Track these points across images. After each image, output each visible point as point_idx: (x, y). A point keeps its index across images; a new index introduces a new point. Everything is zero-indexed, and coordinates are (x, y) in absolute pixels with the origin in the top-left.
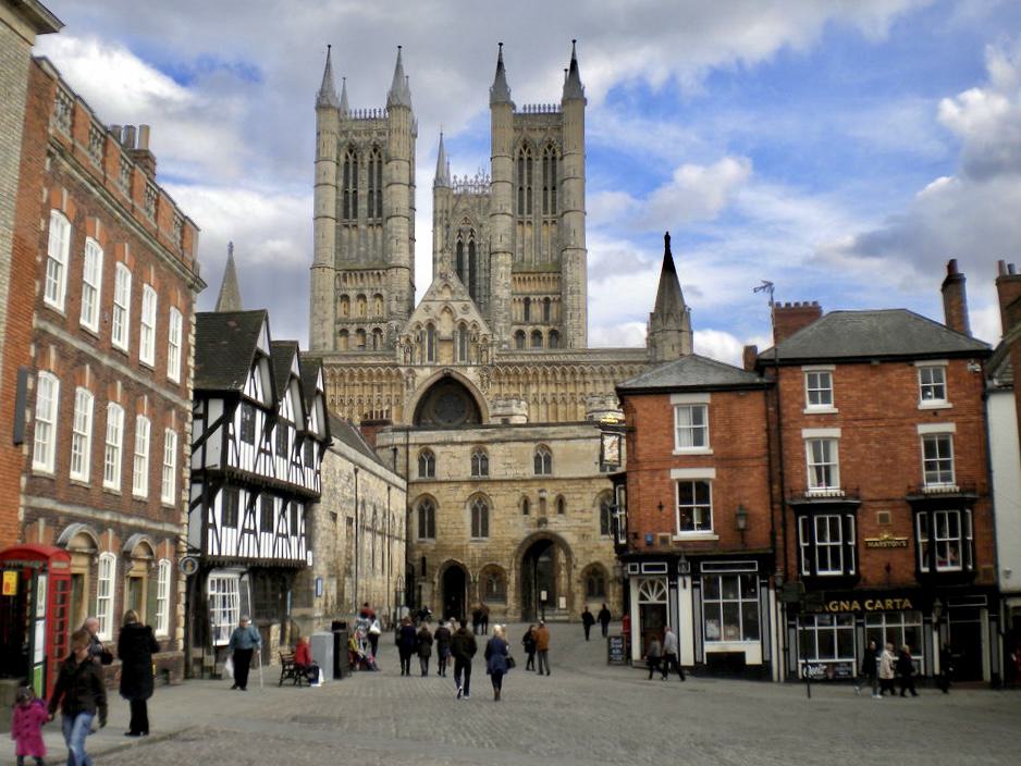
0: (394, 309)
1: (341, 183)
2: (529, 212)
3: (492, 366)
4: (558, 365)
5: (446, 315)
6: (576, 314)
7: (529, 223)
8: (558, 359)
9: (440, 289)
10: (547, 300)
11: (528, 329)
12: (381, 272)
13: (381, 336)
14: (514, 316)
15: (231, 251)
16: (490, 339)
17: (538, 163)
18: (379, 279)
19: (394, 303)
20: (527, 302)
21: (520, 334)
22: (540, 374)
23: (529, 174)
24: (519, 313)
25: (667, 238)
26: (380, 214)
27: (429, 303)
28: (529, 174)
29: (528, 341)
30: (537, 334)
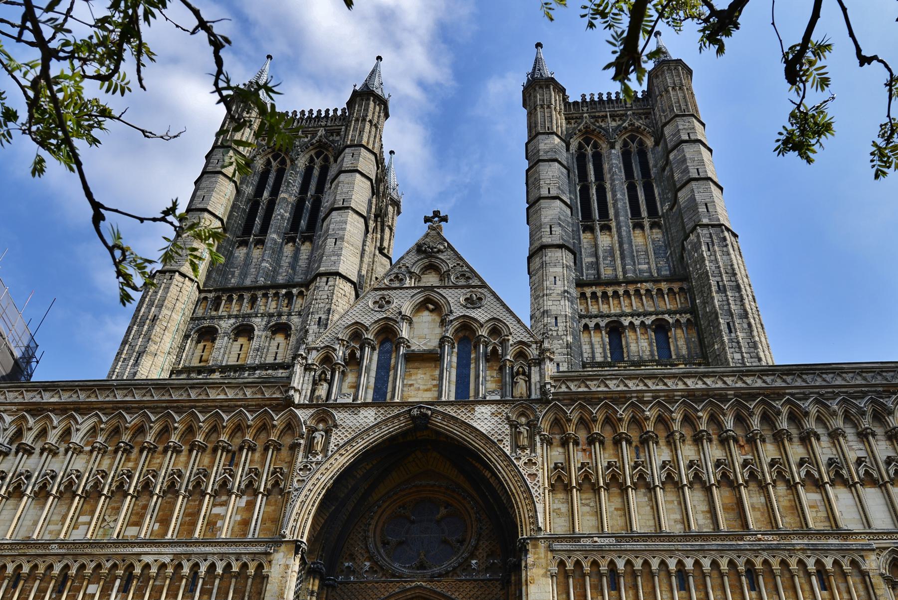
1: (249, 190)
2: (604, 213)
3: (544, 400)
4: (724, 399)
5: (426, 318)
7: (606, 228)
8: (720, 385)
9: (416, 270)
12: (295, 291)
14: (585, 355)
16: (533, 352)
17: (613, 151)
18: (290, 303)
20: (615, 330)
22: (678, 416)
24: (598, 350)
27: (385, 292)
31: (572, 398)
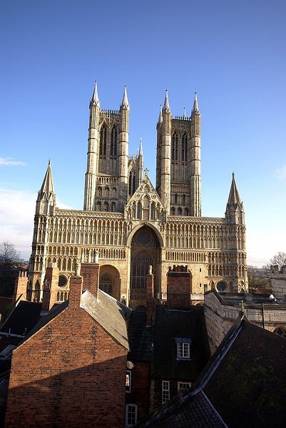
0: (121, 195)
11: (177, 207)
20: (176, 195)
21: (173, 209)
23: (177, 144)
26: (115, 154)
28: (177, 144)
29: (176, 210)
31: (169, 222)
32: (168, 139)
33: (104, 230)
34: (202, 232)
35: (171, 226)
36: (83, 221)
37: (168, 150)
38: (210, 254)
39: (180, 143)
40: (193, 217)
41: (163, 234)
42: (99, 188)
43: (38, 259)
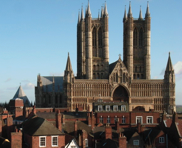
0: (106, 69)
2: (136, 45)
6: (148, 71)
10: (141, 67)
12: (103, 59)
13: (103, 75)
15: (69, 55)
19: (106, 67)
20: (136, 67)
21: (134, 75)
23: (136, 35)
25: (169, 53)
26: (101, 45)
28: (136, 35)
29: (136, 76)
30: (138, 75)
31: (133, 83)
32: (132, 33)
33: (99, 89)
34: (151, 87)
35: (134, 85)
36: (89, 85)
37: (132, 40)
38: (155, 99)
39: (138, 35)
40: (145, 80)
41: (130, 90)
42: (94, 66)
43: (69, 105)
